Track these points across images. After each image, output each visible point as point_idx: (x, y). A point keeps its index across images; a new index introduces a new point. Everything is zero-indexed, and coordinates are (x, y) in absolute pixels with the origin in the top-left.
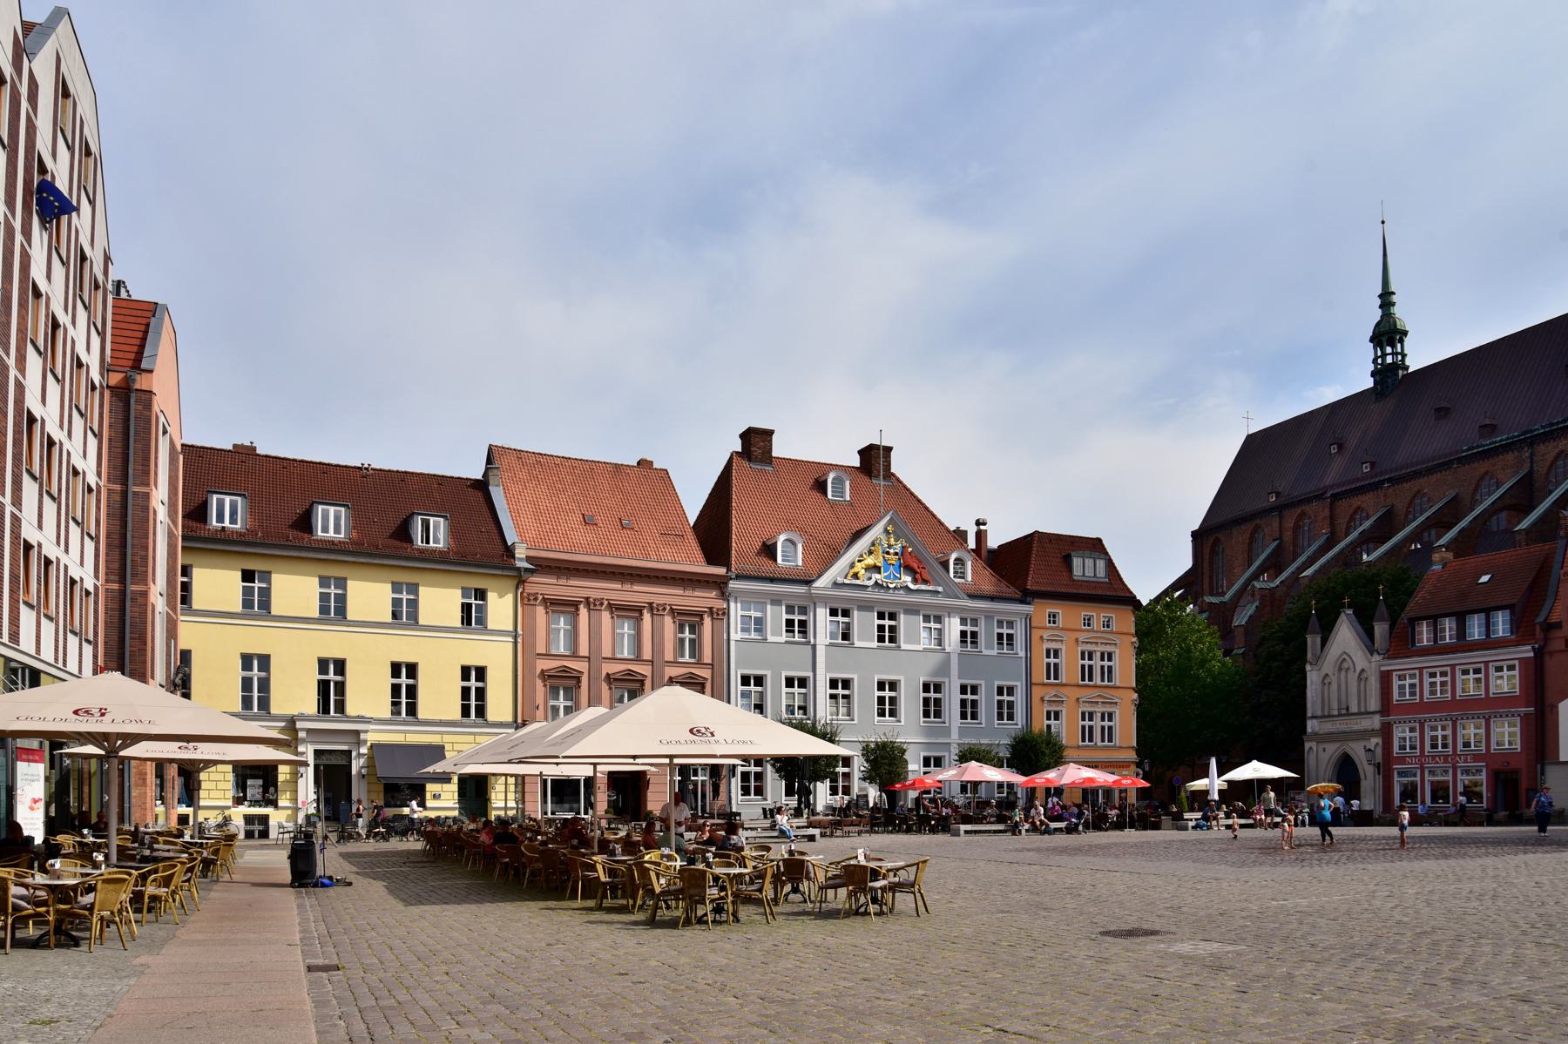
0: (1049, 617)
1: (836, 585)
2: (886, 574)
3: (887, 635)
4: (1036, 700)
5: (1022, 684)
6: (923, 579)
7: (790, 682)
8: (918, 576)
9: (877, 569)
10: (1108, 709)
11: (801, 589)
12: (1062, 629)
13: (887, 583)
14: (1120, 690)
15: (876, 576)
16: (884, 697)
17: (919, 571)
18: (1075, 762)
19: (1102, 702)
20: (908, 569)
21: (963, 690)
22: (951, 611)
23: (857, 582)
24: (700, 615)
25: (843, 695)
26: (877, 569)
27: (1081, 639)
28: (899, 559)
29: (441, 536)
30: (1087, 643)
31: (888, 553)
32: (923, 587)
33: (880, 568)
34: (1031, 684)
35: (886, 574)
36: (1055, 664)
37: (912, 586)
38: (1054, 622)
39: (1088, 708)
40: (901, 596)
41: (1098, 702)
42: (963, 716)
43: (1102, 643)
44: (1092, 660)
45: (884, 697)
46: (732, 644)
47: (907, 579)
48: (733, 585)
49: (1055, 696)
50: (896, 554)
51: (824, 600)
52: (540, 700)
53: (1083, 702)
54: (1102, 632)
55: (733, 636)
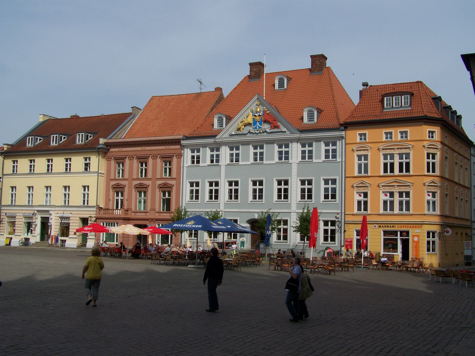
0: (429, 133)
1: (231, 135)
2: (254, 127)
5: (339, 178)
6: (274, 126)
9: (249, 124)
10: (403, 189)
13: (255, 130)
14: (371, 178)
15: (248, 128)
16: (328, 188)
17: (272, 122)
19: (397, 186)
20: (265, 121)
22: (292, 141)
23: (240, 133)
27: (381, 148)
28: (262, 118)
30: (387, 149)
31: (255, 116)
32: (275, 130)
33: (251, 124)
34: (346, 177)
35: (254, 127)
37: (268, 130)
40: (265, 137)
41: (394, 186)
42: (303, 197)
43: (398, 149)
44: (434, 159)
45: (328, 188)
46: (185, 168)
47: (266, 127)
48: (183, 142)
49: (362, 183)
50: (260, 116)
51: (225, 144)
53: (383, 186)
54: (400, 141)
55: (186, 165)
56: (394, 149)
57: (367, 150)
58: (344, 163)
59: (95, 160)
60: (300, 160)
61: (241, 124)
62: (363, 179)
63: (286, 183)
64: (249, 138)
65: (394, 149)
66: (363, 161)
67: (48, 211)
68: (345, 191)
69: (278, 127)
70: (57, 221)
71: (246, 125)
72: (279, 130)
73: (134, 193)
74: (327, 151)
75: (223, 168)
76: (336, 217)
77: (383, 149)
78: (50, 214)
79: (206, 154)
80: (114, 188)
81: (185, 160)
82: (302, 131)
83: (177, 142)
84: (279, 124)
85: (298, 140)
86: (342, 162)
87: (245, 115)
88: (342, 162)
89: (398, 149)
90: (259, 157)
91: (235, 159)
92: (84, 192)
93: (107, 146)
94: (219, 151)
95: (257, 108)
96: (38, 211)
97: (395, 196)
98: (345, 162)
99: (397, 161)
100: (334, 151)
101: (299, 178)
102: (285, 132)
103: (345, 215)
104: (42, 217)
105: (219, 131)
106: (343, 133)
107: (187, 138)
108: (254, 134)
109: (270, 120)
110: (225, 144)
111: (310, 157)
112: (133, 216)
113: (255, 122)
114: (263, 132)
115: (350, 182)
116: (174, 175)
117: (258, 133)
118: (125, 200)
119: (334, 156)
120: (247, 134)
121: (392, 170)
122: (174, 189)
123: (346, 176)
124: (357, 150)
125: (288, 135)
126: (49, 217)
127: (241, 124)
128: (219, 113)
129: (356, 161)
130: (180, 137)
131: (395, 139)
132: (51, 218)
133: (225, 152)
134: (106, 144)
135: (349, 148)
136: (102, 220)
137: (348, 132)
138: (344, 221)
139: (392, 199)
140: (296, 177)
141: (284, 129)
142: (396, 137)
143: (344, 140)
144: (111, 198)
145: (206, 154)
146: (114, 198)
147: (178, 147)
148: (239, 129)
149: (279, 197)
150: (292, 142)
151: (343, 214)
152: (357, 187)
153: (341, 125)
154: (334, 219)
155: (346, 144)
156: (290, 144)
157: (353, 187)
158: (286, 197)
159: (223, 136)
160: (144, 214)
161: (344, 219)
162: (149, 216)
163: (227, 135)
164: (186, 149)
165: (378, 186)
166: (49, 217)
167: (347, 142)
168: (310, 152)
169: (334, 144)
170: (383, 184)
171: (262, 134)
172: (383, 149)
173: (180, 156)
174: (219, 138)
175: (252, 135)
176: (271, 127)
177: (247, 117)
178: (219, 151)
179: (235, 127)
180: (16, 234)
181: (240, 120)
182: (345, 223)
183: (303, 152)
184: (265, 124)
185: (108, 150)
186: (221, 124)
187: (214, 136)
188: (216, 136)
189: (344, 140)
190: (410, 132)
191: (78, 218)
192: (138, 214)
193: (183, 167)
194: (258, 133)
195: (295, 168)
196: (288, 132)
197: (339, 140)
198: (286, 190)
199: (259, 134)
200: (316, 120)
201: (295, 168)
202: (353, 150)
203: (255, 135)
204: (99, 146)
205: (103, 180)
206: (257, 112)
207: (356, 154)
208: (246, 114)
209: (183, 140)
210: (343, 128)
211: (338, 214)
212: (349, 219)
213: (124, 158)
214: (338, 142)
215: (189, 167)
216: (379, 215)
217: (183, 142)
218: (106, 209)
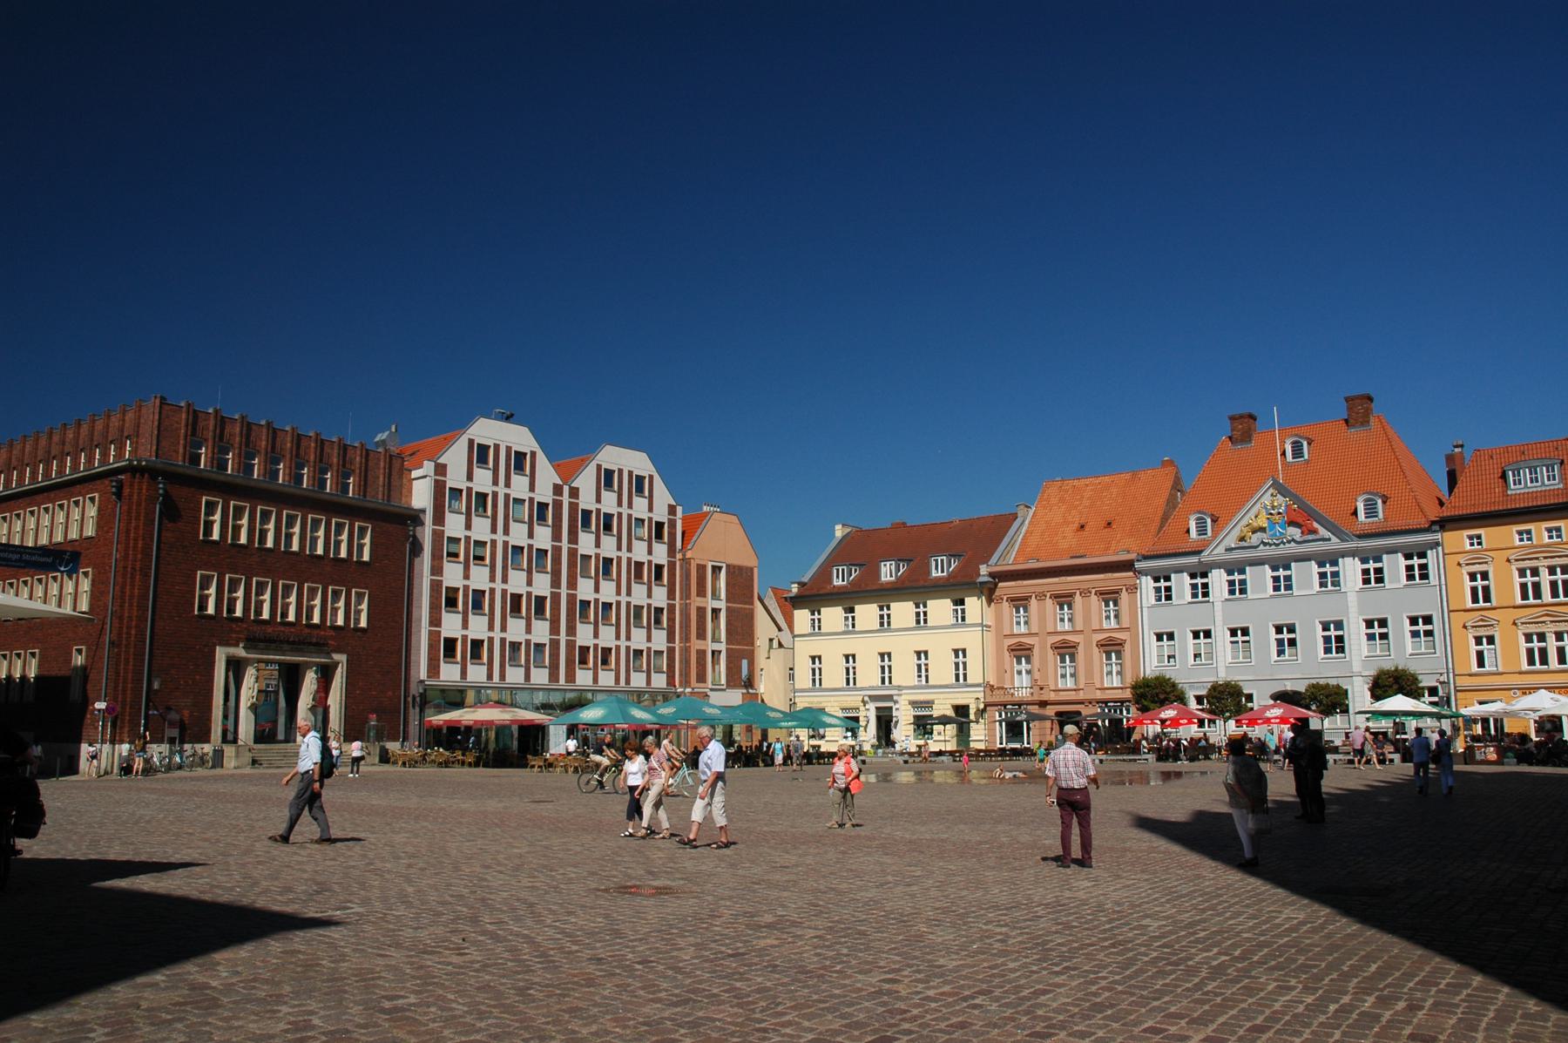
1: (1229, 550)
3: (1282, 585)
4: (1457, 626)
7: (1196, 635)
8: (1304, 528)
9: (1262, 530)
11: (1194, 560)
12: (1486, 550)
18: (1545, 688)
19: (1552, 622)
20: (1292, 523)
21: (1369, 624)
24: (1117, 592)
25: (1425, 631)
26: (1262, 530)
27: (1513, 557)
29: (934, 563)
31: (1271, 514)
32: (1310, 537)
34: (1449, 611)
36: (1483, 587)
37: (1298, 537)
38: (1559, 536)
39: (1532, 629)
41: (1544, 622)
43: (1545, 558)
47: (1295, 532)
49: (1482, 620)
50: (1279, 513)
52: (1007, 667)
53: (1523, 623)
54: (1548, 545)
56: (1537, 558)
57: (1486, 563)
58: (1444, 587)
59: (973, 604)
60: (1361, 586)
61: (1245, 530)
62: (1483, 613)
63: (1339, 625)
64: (1263, 552)
65: (1537, 558)
66: (1479, 583)
67: (891, 696)
68: (1450, 635)
69: (1315, 532)
70: (909, 713)
71: (1254, 532)
72: (1318, 537)
73: (1051, 656)
74: (1410, 568)
75: (1218, 606)
76: (1438, 681)
77: (1517, 560)
78: (896, 702)
79: (1182, 584)
80: (1012, 650)
81: (1144, 596)
82: (1361, 537)
83: (1127, 566)
84: (1316, 525)
85: (1352, 554)
86: (1440, 585)
87: (1252, 514)
88: (1440, 585)
89: (1545, 558)
90: (1282, 585)
91: (1238, 589)
92: (957, 660)
93: (994, 578)
94: (1207, 577)
95: (1273, 502)
96: (870, 697)
97: (1548, 639)
98: (1446, 585)
99: (1545, 579)
100: (1423, 567)
101: (1361, 618)
102: (1329, 539)
103: (1455, 675)
104: (877, 708)
105: (1206, 544)
106: (1438, 536)
107: (1146, 558)
108: (1271, 545)
109: (1300, 521)
110: (1218, 565)
111: (1380, 580)
112: (1052, 697)
113: (1273, 524)
114: (1289, 542)
115: (1459, 618)
116: (1125, 623)
117: (1278, 545)
118: (1036, 670)
119: (1424, 576)
120: (1258, 546)
121: (1537, 595)
122: (1127, 647)
123: (1451, 609)
124: (1467, 564)
125: (1335, 543)
126: (891, 708)
127: (1245, 530)
128: (1199, 512)
129: (1468, 584)
130: (1132, 556)
131: (1537, 540)
132: (897, 709)
133: (1218, 579)
134: (991, 575)
135: (1452, 560)
136: (996, 708)
137: (1447, 535)
138: (1455, 687)
139: (1543, 644)
140: (1356, 615)
141: (1327, 534)
142: (1540, 537)
143: (1440, 548)
144: (1007, 667)
145: (1182, 584)
146: (1012, 668)
147: (1131, 574)
148: (1242, 539)
149: (1327, 650)
150: (1343, 557)
151: (1451, 675)
152: (1473, 627)
153: (1433, 523)
154: (1435, 684)
155: (1444, 554)
156: (1340, 560)
157: (1465, 627)
158: (1341, 649)
159: (1216, 552)
160: (1074, 693)
161: (1455, 683)
162: (1081, 696)
163: (1221, 549)
164: (1144, 579)
165: (1515, 624)
166: (891, 708)
167: (1446, 551)
168: (1379, 571)
169: (1422, 555)
170: (1523, 620)
171: (1287, 545)
172: (1517, 560)
173: (1133, 589)
174: (1206, 556)
175: (1268, 547)
176: (1302, 533)
177: (1256, 517)
178: (1207, 577)
179: (1236, 533)
180: (827, 738)
181: (1244, 522)
182: (1457, 691)
183: (1366, 572)
184: (1291, 528)
185: (996, 585)
186: (1202, 530)
187: (1198, 553)
188: (1201, 551)
189: (1440, 548)
190: (1566, 528)
191: (950, 707)
192: (1061, 693)
193: (1142, 608)
194: (1278, 545)
195: (1352, 599)
196: (1335, 540)
197: (1432, 549)
198: (1340, 639)
199: (1282, 546)
200: (1381, 515)
201: (1352, 599)
202: (1459, 564)
203: (1273, 547)
204: (981, 579)
205: (990, 637)
206: (1273, 507)
207: (1465, 570)
208: (1254, 510)
209: (1138, 561)
210: (1437, 528)
211: (1441, 674)
212: (1464, 682)
213: (1027, 599)
214: (1429, 552)
215: (1153, 606)
216: (1521, 673)
217: (1137, 565)
218: (998, 688)
